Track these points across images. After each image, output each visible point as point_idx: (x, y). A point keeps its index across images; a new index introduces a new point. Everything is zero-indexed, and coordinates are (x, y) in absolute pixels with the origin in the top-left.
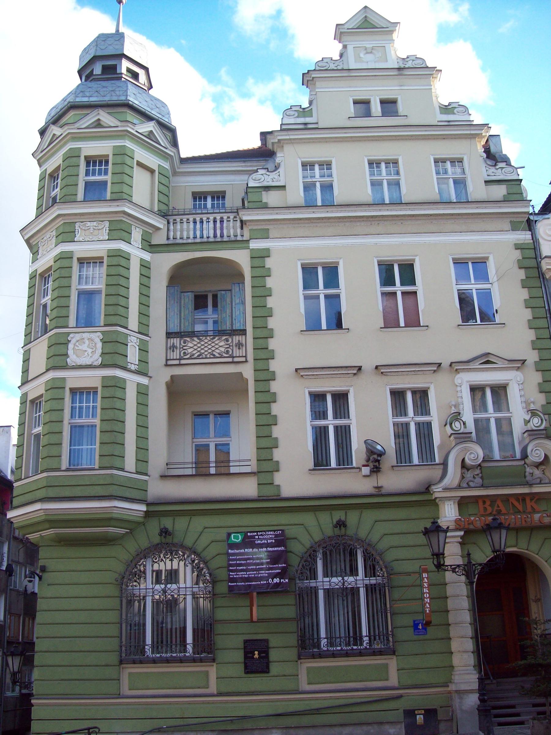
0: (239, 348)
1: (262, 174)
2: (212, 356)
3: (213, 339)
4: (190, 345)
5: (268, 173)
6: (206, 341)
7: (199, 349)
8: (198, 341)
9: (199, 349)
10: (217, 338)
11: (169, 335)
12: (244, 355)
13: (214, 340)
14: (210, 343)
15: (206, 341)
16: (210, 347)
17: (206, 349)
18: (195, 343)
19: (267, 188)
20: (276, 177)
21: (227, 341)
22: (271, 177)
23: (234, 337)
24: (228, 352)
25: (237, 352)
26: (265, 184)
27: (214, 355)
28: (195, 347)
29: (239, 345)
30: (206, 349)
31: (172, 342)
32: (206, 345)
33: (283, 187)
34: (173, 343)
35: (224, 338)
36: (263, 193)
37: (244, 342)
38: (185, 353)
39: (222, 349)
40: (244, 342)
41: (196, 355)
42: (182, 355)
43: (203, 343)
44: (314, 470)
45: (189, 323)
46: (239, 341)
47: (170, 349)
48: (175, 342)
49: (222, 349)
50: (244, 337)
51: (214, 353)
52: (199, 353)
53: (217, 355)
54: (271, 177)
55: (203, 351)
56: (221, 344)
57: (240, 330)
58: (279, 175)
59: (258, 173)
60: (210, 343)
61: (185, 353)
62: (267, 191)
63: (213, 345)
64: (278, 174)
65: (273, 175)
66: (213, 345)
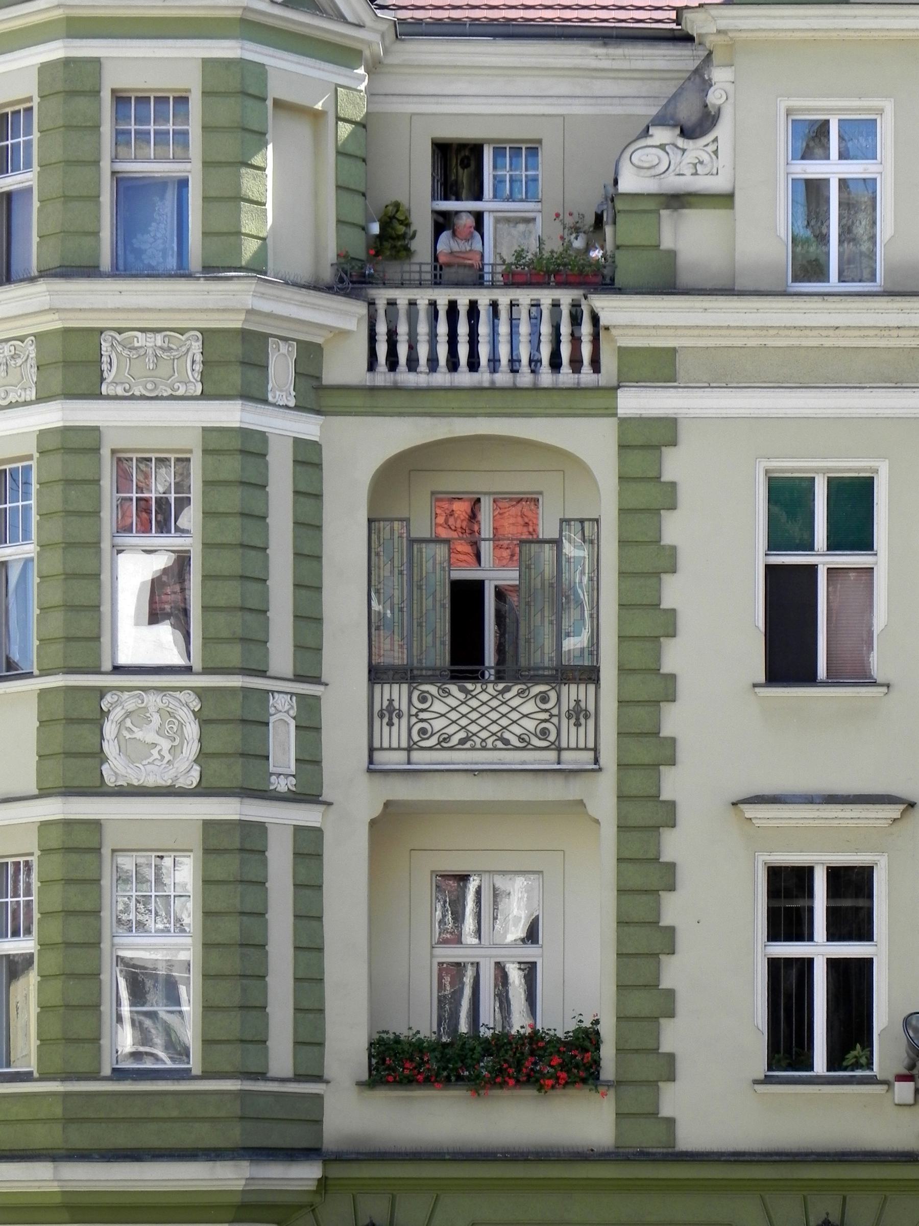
0: (578, 725)
1: (662, 147)
2: (499, 744)
3: (502, 692)
4: (439, 707)
5: (681, 142)
6: (484, 697)
7: (464, 722)
8: (462, 696)
9: (464, 722)
10: (515, 690)
11: (377, 674)
12: (591, 745)
13: (508, 696)
14: (494, 703)
15: (484, 697)
16: (494, 716)
17: (484, 722)
18: (454, 703)
19: (678, 200)
20: (705, 157)
21: (544, 699)
22: (690, 157)
23: (565, 689)
24: (545, 733)
25: (571, 735)
26: (673, 183)
27: (506, 742)
28: (454, 716)
29: (578, 714)
30: (484, 722)
31: (386, 696)
32: (484, 709)
33: (726, 199)
34: (391, 701)
35: (536, 689)
36: (664, 213)
37: (591, 708)
38: (423, 731)
39: (530, 725)
40: (591, 708)
41: (454, 741)
42: (416, 738)
43: (474, 703)
44: (767, 1080)
45: (434, 637)
46: (578, 702)
47: (382, 717)
48: (395, 696)
49: (530, 725)
50: (592, 688)
51: (507, 735)
52: (462, 734)
53: (515, 742)
54: (690, 157)
55: (474, 728)
56: (525, 709)
57: (582, 669)
58: (716, 152)
59: (649, 141)
60: (494, 703)
61: (423, 731)
62: (676, 209)
63: (504, 709)
64: (712, 148)
65: (696, 149)
66: (504, 709)
